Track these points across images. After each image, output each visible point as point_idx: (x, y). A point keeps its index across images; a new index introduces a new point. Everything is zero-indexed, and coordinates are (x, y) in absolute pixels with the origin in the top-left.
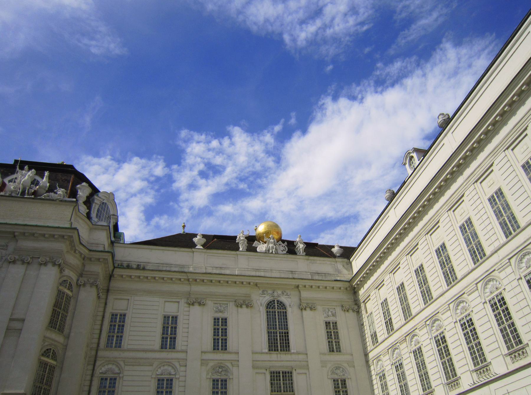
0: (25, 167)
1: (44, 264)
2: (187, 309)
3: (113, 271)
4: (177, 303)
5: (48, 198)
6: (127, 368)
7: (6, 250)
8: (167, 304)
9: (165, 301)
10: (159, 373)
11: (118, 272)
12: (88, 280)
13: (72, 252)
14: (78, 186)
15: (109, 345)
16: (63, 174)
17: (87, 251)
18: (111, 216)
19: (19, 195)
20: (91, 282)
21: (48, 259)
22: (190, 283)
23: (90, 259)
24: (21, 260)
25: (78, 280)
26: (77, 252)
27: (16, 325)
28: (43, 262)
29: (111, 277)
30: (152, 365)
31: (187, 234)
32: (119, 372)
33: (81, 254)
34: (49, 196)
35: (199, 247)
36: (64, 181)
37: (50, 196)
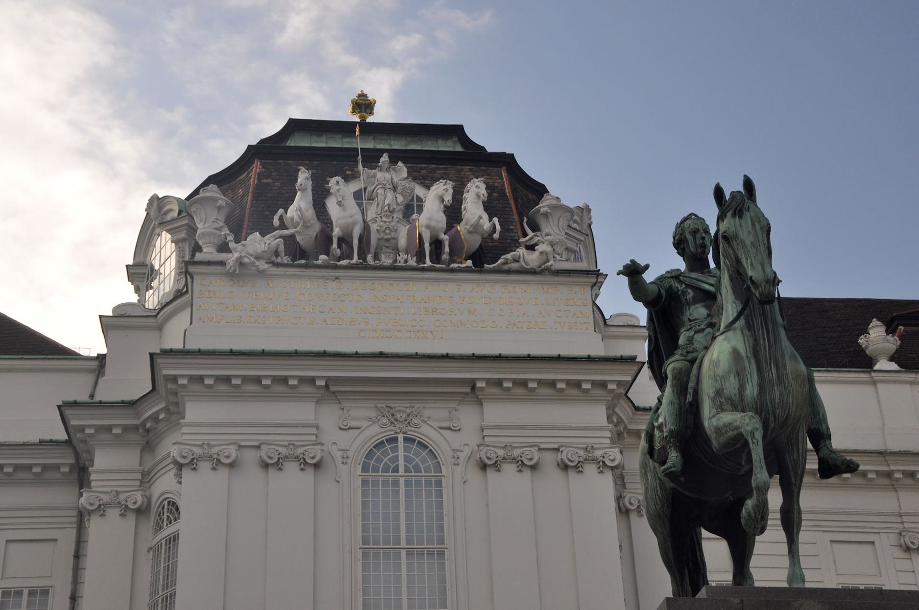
0: (382, 160)
1: (576, 467)
2: (905, 564)
5: (515, 266)
16: (475, 168)
19: (428, 263)
22: (894, 483)
34: (516, 260)
35: (883, 364)
37: (521, 259)
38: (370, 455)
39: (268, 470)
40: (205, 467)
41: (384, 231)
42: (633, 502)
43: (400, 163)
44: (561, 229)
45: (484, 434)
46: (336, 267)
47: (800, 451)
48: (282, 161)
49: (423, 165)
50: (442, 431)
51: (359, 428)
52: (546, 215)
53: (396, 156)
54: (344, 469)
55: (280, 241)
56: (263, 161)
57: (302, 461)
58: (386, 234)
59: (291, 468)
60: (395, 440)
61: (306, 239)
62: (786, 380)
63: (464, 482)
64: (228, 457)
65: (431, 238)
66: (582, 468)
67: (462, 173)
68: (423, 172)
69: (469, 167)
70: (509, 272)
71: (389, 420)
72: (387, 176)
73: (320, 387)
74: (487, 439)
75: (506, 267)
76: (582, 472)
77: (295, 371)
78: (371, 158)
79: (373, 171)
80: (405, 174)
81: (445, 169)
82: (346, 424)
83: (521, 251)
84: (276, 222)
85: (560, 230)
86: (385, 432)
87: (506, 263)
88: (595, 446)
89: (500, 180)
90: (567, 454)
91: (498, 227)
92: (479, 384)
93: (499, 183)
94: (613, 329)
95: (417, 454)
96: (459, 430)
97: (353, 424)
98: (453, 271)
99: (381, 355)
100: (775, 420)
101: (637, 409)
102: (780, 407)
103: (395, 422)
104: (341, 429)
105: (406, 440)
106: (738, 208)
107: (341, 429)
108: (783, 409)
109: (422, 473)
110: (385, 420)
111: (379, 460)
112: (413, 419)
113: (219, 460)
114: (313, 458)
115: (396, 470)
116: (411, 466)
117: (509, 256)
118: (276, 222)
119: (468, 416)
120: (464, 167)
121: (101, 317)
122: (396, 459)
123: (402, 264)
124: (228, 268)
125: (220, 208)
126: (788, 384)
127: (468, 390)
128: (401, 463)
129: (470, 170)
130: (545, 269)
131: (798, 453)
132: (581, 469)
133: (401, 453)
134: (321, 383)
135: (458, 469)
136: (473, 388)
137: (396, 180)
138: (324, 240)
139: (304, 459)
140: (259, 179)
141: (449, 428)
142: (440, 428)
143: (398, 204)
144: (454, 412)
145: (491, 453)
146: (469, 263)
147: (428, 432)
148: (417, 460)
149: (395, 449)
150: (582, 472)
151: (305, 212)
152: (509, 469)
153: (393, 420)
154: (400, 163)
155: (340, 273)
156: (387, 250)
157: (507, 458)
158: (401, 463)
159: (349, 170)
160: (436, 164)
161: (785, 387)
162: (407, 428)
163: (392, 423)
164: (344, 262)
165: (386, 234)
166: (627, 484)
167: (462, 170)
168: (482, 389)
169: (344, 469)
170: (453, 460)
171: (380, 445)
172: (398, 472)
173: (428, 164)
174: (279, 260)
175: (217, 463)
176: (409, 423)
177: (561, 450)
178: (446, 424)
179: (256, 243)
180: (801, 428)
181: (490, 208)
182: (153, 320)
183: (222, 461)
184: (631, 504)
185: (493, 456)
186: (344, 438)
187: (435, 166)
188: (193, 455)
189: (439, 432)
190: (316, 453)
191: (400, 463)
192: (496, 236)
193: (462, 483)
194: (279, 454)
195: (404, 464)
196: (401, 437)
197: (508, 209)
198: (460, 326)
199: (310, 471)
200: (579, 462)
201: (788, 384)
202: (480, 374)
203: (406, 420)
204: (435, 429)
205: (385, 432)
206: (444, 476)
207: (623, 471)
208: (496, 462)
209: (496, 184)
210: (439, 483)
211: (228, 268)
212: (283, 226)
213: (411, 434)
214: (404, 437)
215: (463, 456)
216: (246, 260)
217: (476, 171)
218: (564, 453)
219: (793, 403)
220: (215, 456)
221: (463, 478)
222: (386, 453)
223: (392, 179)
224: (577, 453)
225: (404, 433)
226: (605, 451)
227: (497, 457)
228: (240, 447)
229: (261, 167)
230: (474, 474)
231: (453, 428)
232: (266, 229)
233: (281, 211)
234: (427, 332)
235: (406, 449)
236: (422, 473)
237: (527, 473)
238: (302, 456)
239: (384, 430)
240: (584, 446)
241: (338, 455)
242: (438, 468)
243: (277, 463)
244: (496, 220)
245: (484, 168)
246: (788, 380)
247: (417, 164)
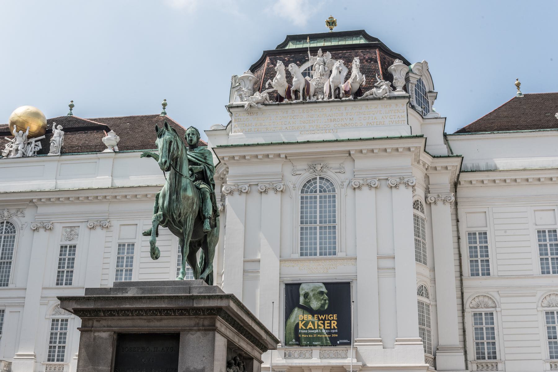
0: (318, 52)
3: (459, 175)
4: (552, 212)
5: (371, 97)
6: (503, 300)
7: (344, 173)
8: (536, 213)
9: (535, 211)
10: (546, 305)
11: (464, 177)
12: (438, 196)
13: (416, 163)
14: (392, 67)
15: (474, 273)
16: (364, 51)
17: (430, 158)
18: (429, 95)
19: (333, 98)
20: (443, 198)
21: (398, 180)
23: (435, 168)
24: (367, 185)
25: (426, 198)
26: (421, 162)
27: (387, 263)
28: (394, 184)
29: (456, 184)
30: (535, 296)
31: (527, 97)
32: (493, 305)
33: (424, 164)
36: (369, 61)
37: (374, 94)
38: (305, 186)
39: (262, 195)
40: (236, 194)
41: (318, 85)
42: (432, 199)
43: (328, 52)
44: (402, 76)
45: (355, 174)
46: (291, 104)
47: (188, 225)
48: (278, 56)
49: (340, 52)
51: (301, 174)
52: (395, 70)
53: (325, 49)
54: (294, 192)
55: (267, 95)
56: (270, 57)
57: (275, 190)
58: (319, 86)
59: (271, 193)
60: (316, 178)
61: (282, 92)
62: (180, 199)
63: (346, 195)
64: (245, 190)
65: (335, 86)
66: (398, 187)
67: (358, 53)
68: (340, 55)
69: (361, 50)
70: (368, 100)
72: (322, 59)
73: (283, 158)
74: (356, 176)
75: (367, 98)
76: (398, 188)
77: (272, 151)
78: (314, 51)
79: (315, 57)
80: (330, 56)
81: (350, 52)
82: (295, 173)
83: (374, 90)
84: (267, 86)
85: (401, 75)
86: (312, 175)
87: (367, 96)
88: (404, 177)
89: (375, 55)
90: (391, 181)
91: (365, 79)
93: (374, 56)
94: (427, 120)
95: (325, 184)
96: (344, 173)
97: (298, 173)
98: (342, 101)
99: (308, 142)
100: (175, 215)
101: (434, 157)
102: (176, 210)
103: (316, 171)
104: (293, 175)
105: (321, 178)
106: (160, 135)
107: (293, 175)
108: (178, 210)
109: (327, 192)
110: (311, 170)
111: (309, 188)
113: (241, 191)
114: (280, 188)
115: (316, 192)
116: (322, 190)
117: (367, 92)
118: (267, 86)
119: (348, 166)
120: (359, 50)
121: (205, 131)
122: (316, 187)
123: (320, 100)
124: (245, 108)
125: (250, 80)
126: (181, 200)
127: (348, 155)
128: (318, 189)
129: (362, 52)
130: (384, 97)
131: (187, 226)
132: (397, 187)
133: (318, 184)
134: (283, 156)
135: (343, 190)
136: (350, 154)
137: (326, 60)
138: (288, 92)
139: (276, 189)
140: (268, 66)
141: (340, 173)
142: (336, 172)
143: (325, 71)
144: (342, 165)
145: (356, 182)
146: (351, 97)
147: (330, 174)
149: (315, 183)
150: (398, 188)
151: (280, 81)
152: (365, 189)
154: (328, 52)
155: (293, 106)
156: (320, 93)
158: (318, 189)
159: (307, 57)
160: (346, 51)
161: (179, 201)
163: (314, 171)
164: (294, 101)
165: (319, 86)
166: (430, 191)
167: (358, 52)
168: (353, 154)
169: (294, 192)
170: (341, 186)
171: (309, 181)
172: (316, 193)
173: (343, 51)
174: (267, 102)
175: (241, 192)
178: (338, 171)
179: (258, 96)
180: (189, 216)
181: (363, 70)
182: (225, 131)
183: (243, 191)
184: (431, 200)
185: (358, 183)
186: (294, 178)
187: (346, 51)
188: (231, 189)
189: (335, 174)
190: (281, 186)
191: (317, 188)
192: (364, 83)
193: (345, 196)
194: (266, 187)
195: (319, 189)
196: (318, 177)
197: (377, 69)
198: (345, 126)
199: (279, 194)
200: (397, 184)
201: (181, 200)
202: (353, 147)
203: (320, 170)
204: (333, 173)
205: (312, 175)
206: (336, 193)
207: (429, 185)
208: (359, 186)
209: (373, 57)
210: (334, 197)
211: (245, 108)
212: (270, 86)
213: (322, 176)
215: (346, 184)
216: (252, 105)
217: (364, 52)
218: (390, 181)
219: (182, 208)
220: (240, 189)
221: (345, 194)
222: (311, 185)
223: (324, 60)
224: (396, 180)
225: (320, 175)
226: (408, 179)
227: (360, 184)
228: (250, 185)
230: (350, 191)
231: (341, 172)
232: (261, 89)
233: (269, 81)
234: (330, 130)
235: (320, 183)
236: (327, 192)
237: (373, 190)
238: (275, 188)
239: (312, 174)
240: (399, 177)
241: (292, 186)
242: (334, 191)
243: (265, 191)
244: (364, 76)
245: (368, 50)
246: (181, 199)
247: (337, 51)
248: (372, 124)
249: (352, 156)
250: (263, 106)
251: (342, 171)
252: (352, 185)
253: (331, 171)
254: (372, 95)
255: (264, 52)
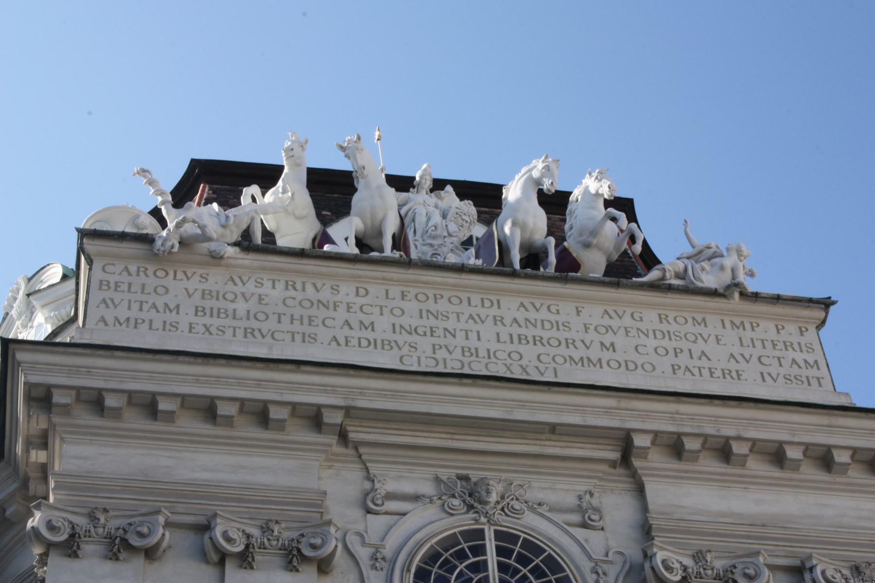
50: (570, 529)
70: (670, 288)
71: (464, 501)
92: (640, 441)
112: (512, 503)
113: (125, 542)
127: (615, 455)
139: (299, 550)
142: (569, 524)
148: (525, 571)
153: (472, 502)
157: (703, 575)
162: (499, 516)
176: (503, 509)
177: (808, 565)
214: (496, 531)
222: (461, 556)
229: (211, 192)
248: (696, 371)
249: (637, 463)
250: (237, 249)
251: (593, 517)
252: (653, 568)
253: (542, 515)
254: (683, 278)
255: (195, 164)
